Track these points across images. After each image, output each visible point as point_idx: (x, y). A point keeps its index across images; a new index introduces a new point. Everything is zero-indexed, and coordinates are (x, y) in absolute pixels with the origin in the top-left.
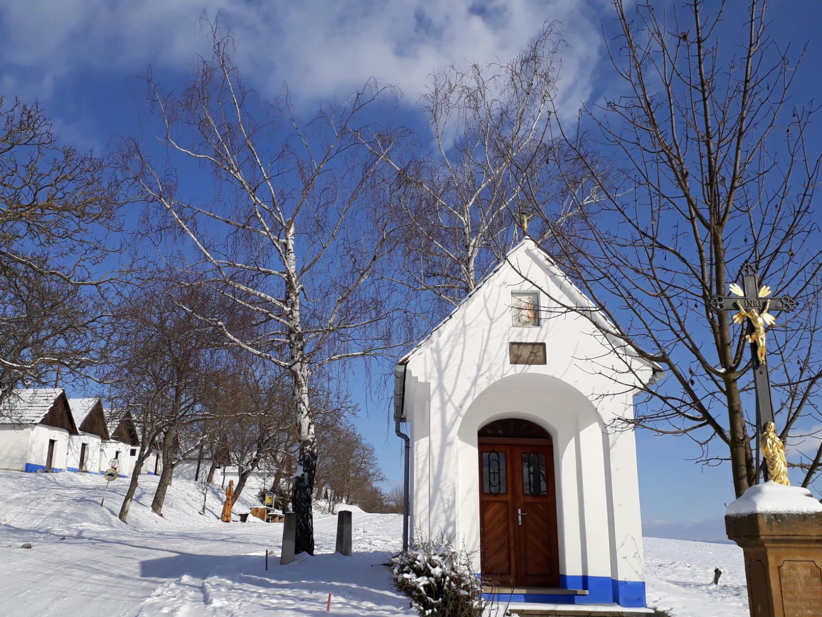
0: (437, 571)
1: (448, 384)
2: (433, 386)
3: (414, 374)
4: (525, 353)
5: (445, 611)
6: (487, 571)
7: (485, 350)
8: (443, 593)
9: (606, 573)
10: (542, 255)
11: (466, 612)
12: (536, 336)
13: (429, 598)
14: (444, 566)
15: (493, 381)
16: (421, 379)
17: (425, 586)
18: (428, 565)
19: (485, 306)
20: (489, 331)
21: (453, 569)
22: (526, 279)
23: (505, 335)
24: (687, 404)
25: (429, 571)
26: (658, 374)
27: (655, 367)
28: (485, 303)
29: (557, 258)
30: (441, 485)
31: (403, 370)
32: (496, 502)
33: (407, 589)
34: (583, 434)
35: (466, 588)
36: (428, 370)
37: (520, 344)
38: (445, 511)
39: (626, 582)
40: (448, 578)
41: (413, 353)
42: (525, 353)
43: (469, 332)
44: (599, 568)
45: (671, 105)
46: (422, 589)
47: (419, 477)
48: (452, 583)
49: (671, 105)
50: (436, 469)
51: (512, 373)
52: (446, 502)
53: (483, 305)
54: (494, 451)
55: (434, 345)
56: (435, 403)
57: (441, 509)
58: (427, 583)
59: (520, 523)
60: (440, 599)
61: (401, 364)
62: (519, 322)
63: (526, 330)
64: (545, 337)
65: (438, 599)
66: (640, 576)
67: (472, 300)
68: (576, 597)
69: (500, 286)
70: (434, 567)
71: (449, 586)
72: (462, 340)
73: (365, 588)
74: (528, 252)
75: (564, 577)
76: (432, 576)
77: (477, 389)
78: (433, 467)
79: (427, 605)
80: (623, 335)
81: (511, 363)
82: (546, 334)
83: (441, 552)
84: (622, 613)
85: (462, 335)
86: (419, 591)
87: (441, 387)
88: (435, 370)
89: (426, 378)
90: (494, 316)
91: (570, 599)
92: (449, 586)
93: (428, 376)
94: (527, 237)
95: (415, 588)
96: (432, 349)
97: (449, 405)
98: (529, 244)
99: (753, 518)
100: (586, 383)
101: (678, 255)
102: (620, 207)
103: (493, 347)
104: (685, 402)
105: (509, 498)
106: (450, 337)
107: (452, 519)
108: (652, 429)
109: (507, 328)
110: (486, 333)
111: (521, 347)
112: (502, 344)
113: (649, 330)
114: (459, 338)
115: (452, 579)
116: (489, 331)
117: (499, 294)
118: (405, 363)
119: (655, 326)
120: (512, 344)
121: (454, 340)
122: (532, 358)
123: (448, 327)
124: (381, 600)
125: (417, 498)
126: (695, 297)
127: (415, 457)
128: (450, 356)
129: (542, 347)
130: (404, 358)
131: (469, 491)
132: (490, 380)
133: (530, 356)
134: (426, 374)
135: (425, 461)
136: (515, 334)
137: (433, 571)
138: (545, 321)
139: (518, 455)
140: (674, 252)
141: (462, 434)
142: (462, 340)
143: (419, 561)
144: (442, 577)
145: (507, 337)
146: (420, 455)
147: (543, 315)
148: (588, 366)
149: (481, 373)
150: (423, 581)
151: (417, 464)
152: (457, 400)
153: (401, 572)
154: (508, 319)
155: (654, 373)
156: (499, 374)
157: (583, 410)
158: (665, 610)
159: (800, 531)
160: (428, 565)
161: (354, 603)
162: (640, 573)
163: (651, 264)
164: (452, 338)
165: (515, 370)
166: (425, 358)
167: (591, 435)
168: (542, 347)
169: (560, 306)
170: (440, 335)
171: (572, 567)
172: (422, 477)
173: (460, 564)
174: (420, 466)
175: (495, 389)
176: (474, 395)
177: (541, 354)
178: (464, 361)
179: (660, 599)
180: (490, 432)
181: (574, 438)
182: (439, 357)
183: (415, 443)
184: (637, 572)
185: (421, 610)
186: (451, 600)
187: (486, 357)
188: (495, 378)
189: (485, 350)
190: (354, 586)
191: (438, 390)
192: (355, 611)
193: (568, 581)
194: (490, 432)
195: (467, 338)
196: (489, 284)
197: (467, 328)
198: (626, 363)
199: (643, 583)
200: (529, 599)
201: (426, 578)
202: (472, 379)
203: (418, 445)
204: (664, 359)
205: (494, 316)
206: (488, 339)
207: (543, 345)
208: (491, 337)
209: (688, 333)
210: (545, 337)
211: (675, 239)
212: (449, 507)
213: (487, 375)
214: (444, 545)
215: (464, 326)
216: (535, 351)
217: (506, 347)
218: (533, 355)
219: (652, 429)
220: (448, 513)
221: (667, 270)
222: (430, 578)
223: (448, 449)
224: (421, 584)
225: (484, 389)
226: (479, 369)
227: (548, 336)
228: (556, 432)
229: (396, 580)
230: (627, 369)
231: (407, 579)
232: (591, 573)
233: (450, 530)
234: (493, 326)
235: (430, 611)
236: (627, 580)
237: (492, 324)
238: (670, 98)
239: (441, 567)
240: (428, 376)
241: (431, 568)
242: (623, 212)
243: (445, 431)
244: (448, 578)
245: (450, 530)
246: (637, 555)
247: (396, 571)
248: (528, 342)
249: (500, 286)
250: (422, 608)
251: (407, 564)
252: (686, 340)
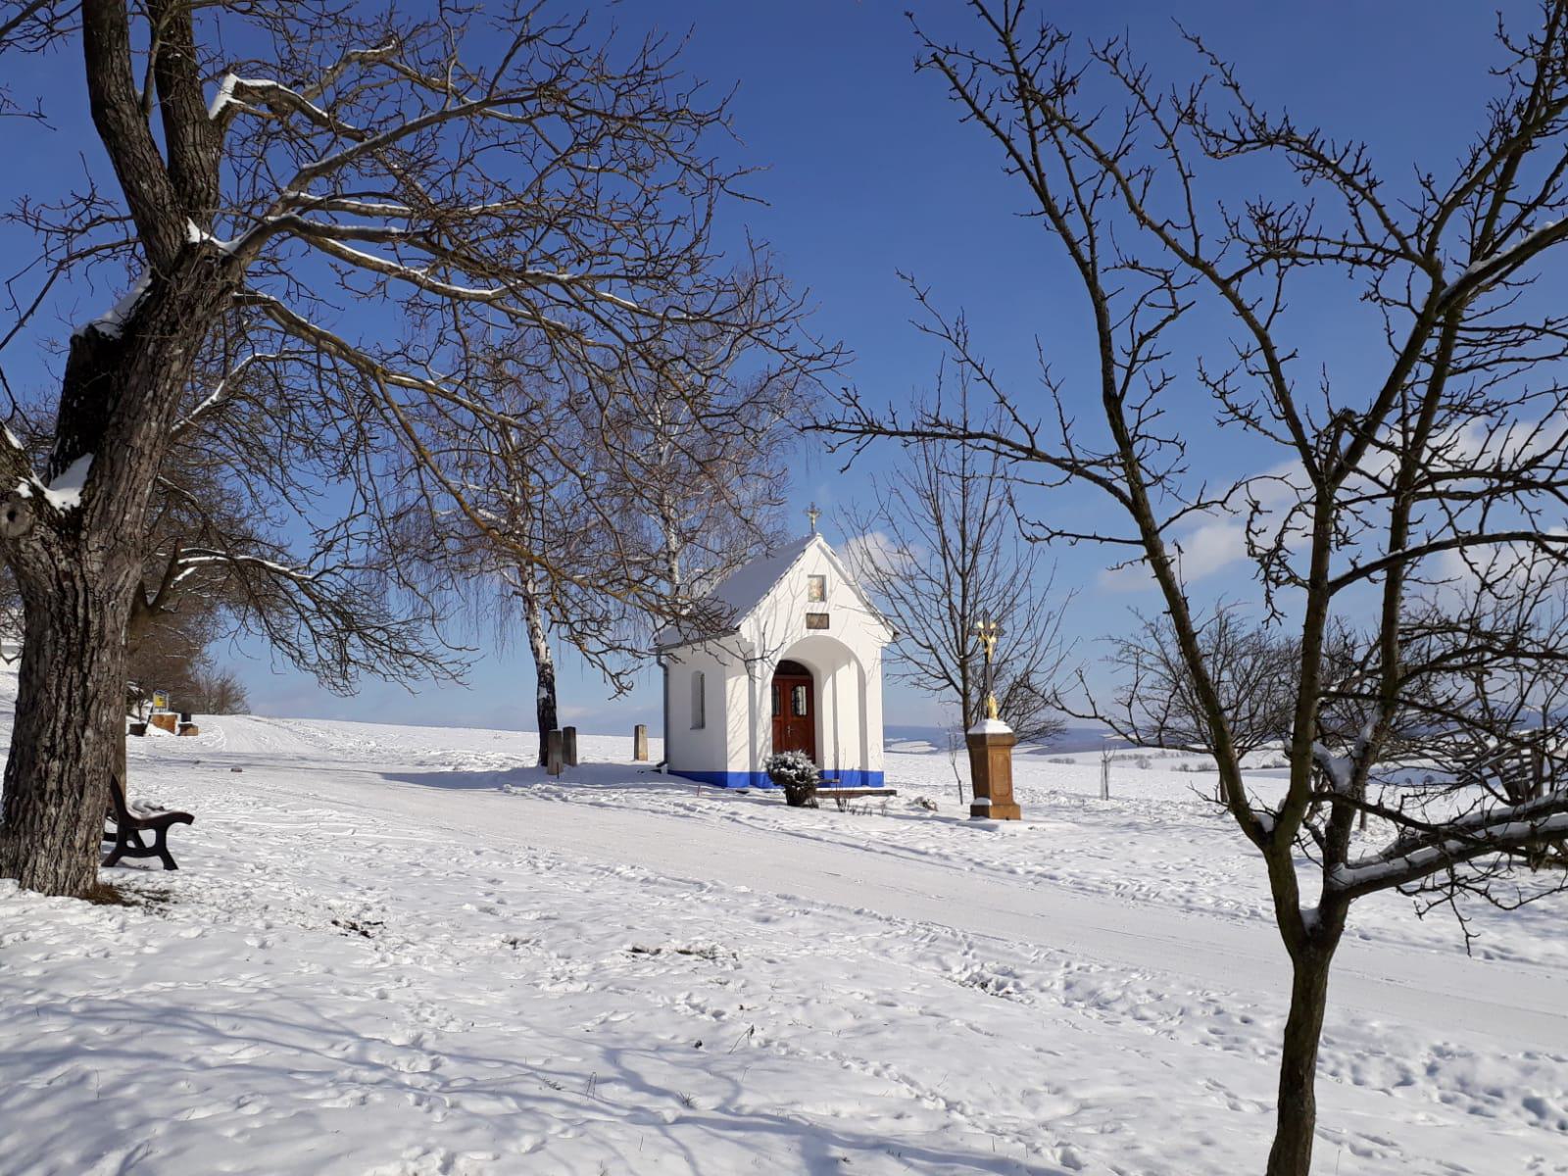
0: (801, 766)
4: (815, 620)
42: (815, 620)
44: (850, 762)
62: (812, 600)
74: (819, 546)
99: (984, 736)
103: (794, 618)
123: (766, 603)
150: (793, 772)
154: (805, 597)
157: (846, 655)
159: (1001, 741)
167: (847, 676)
217: (803, 617)
228: (819, 672)
232: (841, 768)
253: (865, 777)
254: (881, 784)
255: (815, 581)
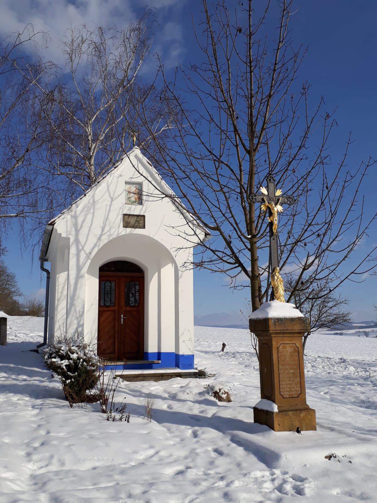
0: (75, 356)
1: (82, 239)
2: (72, 240)
3: (59, 232)
4: (132, 221)
5: (79, 380)
6: (101, 352)
7: (107, 219)
8: (78, 369)
9: (173, 350)
10: (145, 160)
11: (92, 379)
12: (139, 211)
13: (69, 373)
14: (79, 353)
15: (111, 238)
16: (64, 235)
17: (66, 366)
18: (69, 353)
19: (108, 190)
20: (110, 206)
21: (85, 354)
22: (142, 175)
23: (120, 209)
24: (228, 255)
25: (69, 356)
26: (208, 236)
27: (206, 232)
28: (108, 187)
29: (156, 163)
30: (75, 302)
31: (51, 229)
32: (108, 311)
33: (55, 368)
34: (163, 270)
35: (93, 365)
36: (69, 229)
37: (129, 215)
38: (77, 318)
39: (183, 355)
40: (81, 360)
41: (59, 218)
42: (132, 221)
43: (97, 206)
44: (168, 347)
45: (229, 73)
46: (64, 367)
47: (59, 297)
48: (85, 363)
49: (229, 73)
50: (72, 292)
51: (124, 233)
52: (78, 312)
53: (107, 189)
54: (108, 280)
55: (73, 213)
56: (73, 250)
57: (75, 317)
58: (68, 363)
59: (122, 323)
60: (76, 373)
61: (51, 224)
62: (129, 201)
63: (133, 207)
64: (145, 212)
65: (75, 373)
66: (192, 352)
67: (100, 185)
68: (153, 365)
69: (118, 177)
70: (73, 353)
71: (82, 365)
72: (92, 211)
73: (20, 366)
74: (136, 156)
75: (147, 353)
76: (71, 359)
77: (101, 242)
78: (70, 291)
79: (67, 377)
80: (196, 213)
81: (123, 227)
82: (146, 210)
83: (77, 344)
84: (181, 373)
85: (92, 208)
86: (63, 369)
87: (77, 241)
88: (73, 229)
89: (67, 234)
90: (113, 196)
91: (150, 366)
92: (82, 365)
93: (68, 233)
94: (136, 147)
95: (60, 367)
96: (72, 217)
97: (82, 252)
98: (137, 151)
99: (266, 321)
100: (169, 241)
101: (229, 167)
102: (198, 134)
103: (112, 217)
104: (226, 254)
105: (116, 308)
106: (84, 208)
107: (81, 323)
108: (209, 269)
109: (122, 205)
110: (108, 207)
111: (130, 217)
112: (118, 215)
113: (211, 212)
114: (90, 209)
115: (84, 360)
116: (110, 206)
117: (117, 182)
118: (53, 224)
119: (213, 209)
120: (125, 215)
121: (86, 211)
122: (136, 224)
123: (83, 202)
124: (31, 374)
125: (57, 310)
126: (237, 193)
127: (57, 285)
128: (84, 221)
129: (143, 218)
130: (52, 220)
131: (92, 305)
132: (110, 237)
133: (135, 223)
134: (67, 232)
135: (63, 287)
136: (127, 209)
137: (72, 356)
138: (145, 202)
139: (123, 284)
140: (227, 165)
141: (89, 272)
142: (92, 211)
143: (63, 351)
144: (77, 360)
145: (121, 210)
146: (60, 284)
147: (144, 198)
148: (173, 231)
149: (104, 232)
150: (65, 362)
151: (58, 289)
152: (87, 249)
153: (50, 357)
154: (123, 199)
155: (205, 236)
156: (116, 233)
158: (202, 369)
159: (290, 327)
160: (69, 353)
161: (14, 377)
162: (191, 350)
163: (217, 172)
164: (86, 209)
165: (126, 231)
166: (67, 221)
167: (168, 271)
168: (143, 218)
169: (161, 193)
170: (77, 207)
171: (152, 347)
172: (61, 297)
173: (89, 351)
174: (60, 290)
175: (111, 243)
176: (99, 246)
177: (142, 222)
178: (93, 224)
179: (198, 363)
180: (106, 269)
181: (157, 273)
182: (76, 221)
183: (57, 276)
184: (190, 349)
185: (63, 381)
186: (83, 373)
187: (107, 222)
188: (113, 236)
189: (107, 219)
190: (12, 365)
191: (75, 243)
192: (15, 382)
193: (150, 356)
194: (106, 269)
195: (95, 210)
196: (111, 175)
197: (96, 203)
198: (193, 230)
199: (193, 356)
200: (126, 367)
201: (67, 361)
202: (98, 236)
203: (59, 277)
204: (217, 228)
205: (113, 196)
206: (109, 211)
207: (144, 216)
208: (111, 209)
209: (233, 214)
210: (145, 212)
211: (228, 157)
212: (80, 315)
213: (108, 234)
214: (79, 340)
215: (94, 202)
216: (138, 220)
217: (120, 217)
218: (137, 222)
219: (209, 269)
220: (79, 319)
221: (222, 176)
222: (70, 361)
223: (80, 280)
224: (64, 365)
225: (106, 242)
226: (103, 230)
227: (147, 211)
228: (147, 268)
229: (46, 362)
230: (193, 233)
231: (54, 362)
232: (163, 350)
233: (80, 329)
234: (113, 203)
235: (69, 381)
236: (184, 354)
237: (112, 201)
238: (229, 68)
239: (77, 353)
240: (68, 233)
241: (70, 354)
242: (199, 138)
243: (79, 268)
244: (81, 360)
245: (80, 329)
246: (190, 340)
247: (46, 357)
248: (135, 214)
249: (118, 177)
250: (64, 379)
251: (54, 353)
252: (231, 220)
253: (177, 360)
254: (191, 366)
255: (133, 189)
